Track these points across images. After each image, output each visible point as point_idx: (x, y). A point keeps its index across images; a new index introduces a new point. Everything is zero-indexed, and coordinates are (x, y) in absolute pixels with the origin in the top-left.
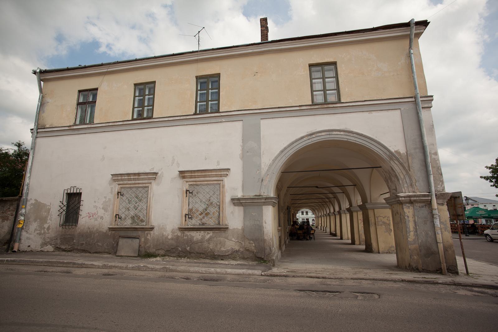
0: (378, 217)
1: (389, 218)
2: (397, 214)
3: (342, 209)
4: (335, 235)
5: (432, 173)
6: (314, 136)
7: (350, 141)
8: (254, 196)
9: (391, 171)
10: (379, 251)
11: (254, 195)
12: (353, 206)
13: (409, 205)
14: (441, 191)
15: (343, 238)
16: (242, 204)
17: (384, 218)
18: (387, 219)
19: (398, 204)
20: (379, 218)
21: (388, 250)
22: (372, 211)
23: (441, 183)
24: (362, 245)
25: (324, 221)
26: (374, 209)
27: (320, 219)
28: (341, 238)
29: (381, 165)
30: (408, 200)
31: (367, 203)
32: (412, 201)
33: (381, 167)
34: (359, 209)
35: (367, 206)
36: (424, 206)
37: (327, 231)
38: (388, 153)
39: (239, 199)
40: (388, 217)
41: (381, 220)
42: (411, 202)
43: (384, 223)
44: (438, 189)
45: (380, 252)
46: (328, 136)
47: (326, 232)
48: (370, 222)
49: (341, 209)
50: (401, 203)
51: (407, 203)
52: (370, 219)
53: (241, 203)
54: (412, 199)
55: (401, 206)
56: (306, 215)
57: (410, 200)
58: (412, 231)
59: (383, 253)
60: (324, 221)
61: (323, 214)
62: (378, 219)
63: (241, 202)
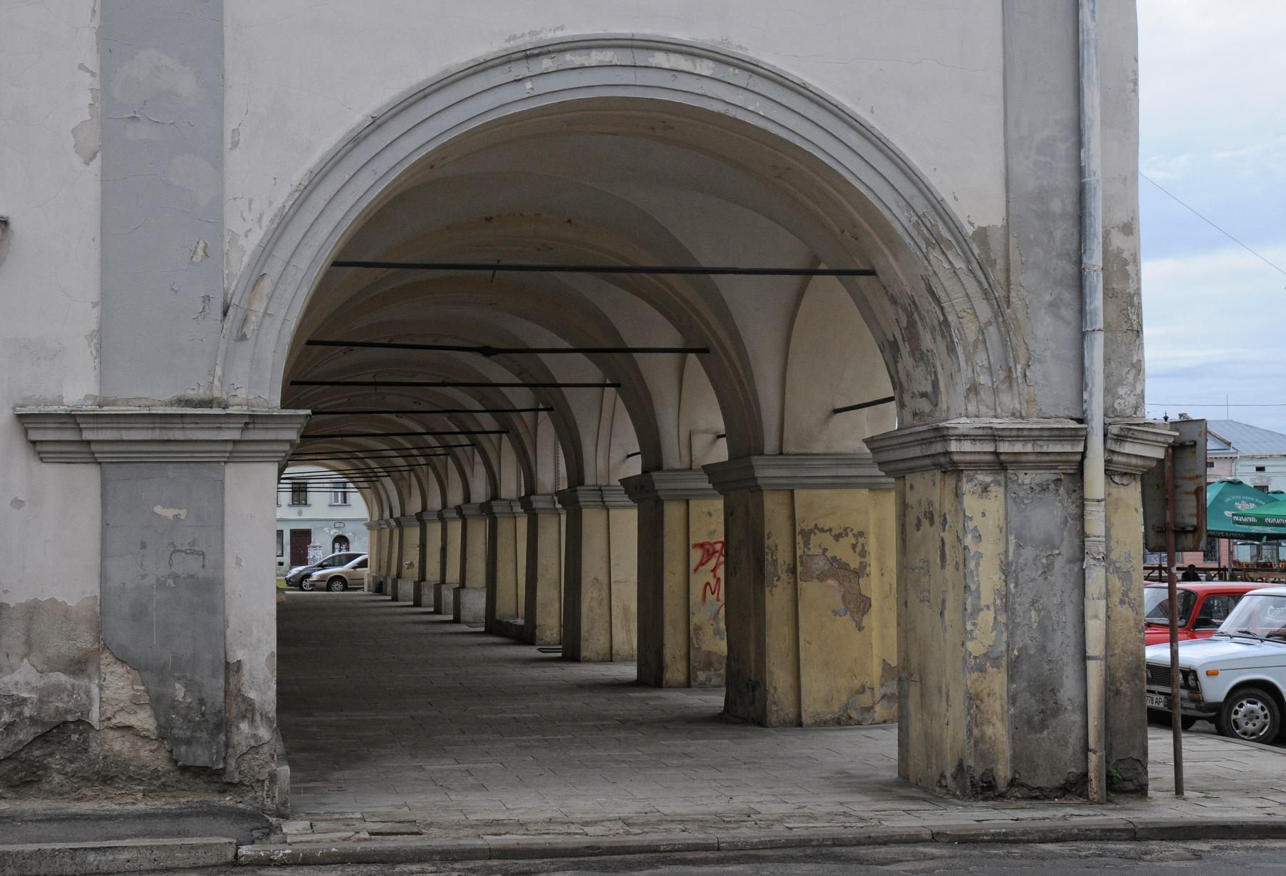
0: (807, 534)
1: (861, 540)
2: (925, 523)
3: (589, 480)
4: (525, 635)
5: (1100, 325)
6: (546, 64)
7: (741, 115)
8: (171, 404)
9: (925, 303)
10: (800, 715)
11: (171, 395)
12: (665, 467)
13: (988, 479)
14: (1129, 411)
16: (94, 448)
17: (837, 537)
18: (854, 547)
19: (938, 475)
20: (814, 539)
21: (846, 707)
22: (782, 498)
23: (1131, 377)
24: (704, 687)
25: (444, 550)
26: (792, 491)
27: (413, 534)
28: (572, 654)
29: (879, 265)
30: (985, 453)
31: (762, 454)
32: (1003, 458)
33: (872, 273)
34: (711, 486)
35: (759, 473)
36: (1052, 486)
37: (466, 614)
38: (920, 204)
39: (72, 419)
40: (861, 534)
41: (825, 550)
42: (1000, 465)
43: (838, 569)
44: (1116, 405)
45: (806, 719)
46: (627, 77)
47: (457, 620)
48: (768, 558)
49: (581, 482)
50: (952, 468)
51: (978, 466)
52: (767, 542)
53: (89, 442)
54: (1004, 447)
55: (951, 481)
56: (296, 509)
57: (996, 454)
58: (988, 607)
59: (822, 724)
60: (444, 550)
62: (807, 544)
63: (88, 435)
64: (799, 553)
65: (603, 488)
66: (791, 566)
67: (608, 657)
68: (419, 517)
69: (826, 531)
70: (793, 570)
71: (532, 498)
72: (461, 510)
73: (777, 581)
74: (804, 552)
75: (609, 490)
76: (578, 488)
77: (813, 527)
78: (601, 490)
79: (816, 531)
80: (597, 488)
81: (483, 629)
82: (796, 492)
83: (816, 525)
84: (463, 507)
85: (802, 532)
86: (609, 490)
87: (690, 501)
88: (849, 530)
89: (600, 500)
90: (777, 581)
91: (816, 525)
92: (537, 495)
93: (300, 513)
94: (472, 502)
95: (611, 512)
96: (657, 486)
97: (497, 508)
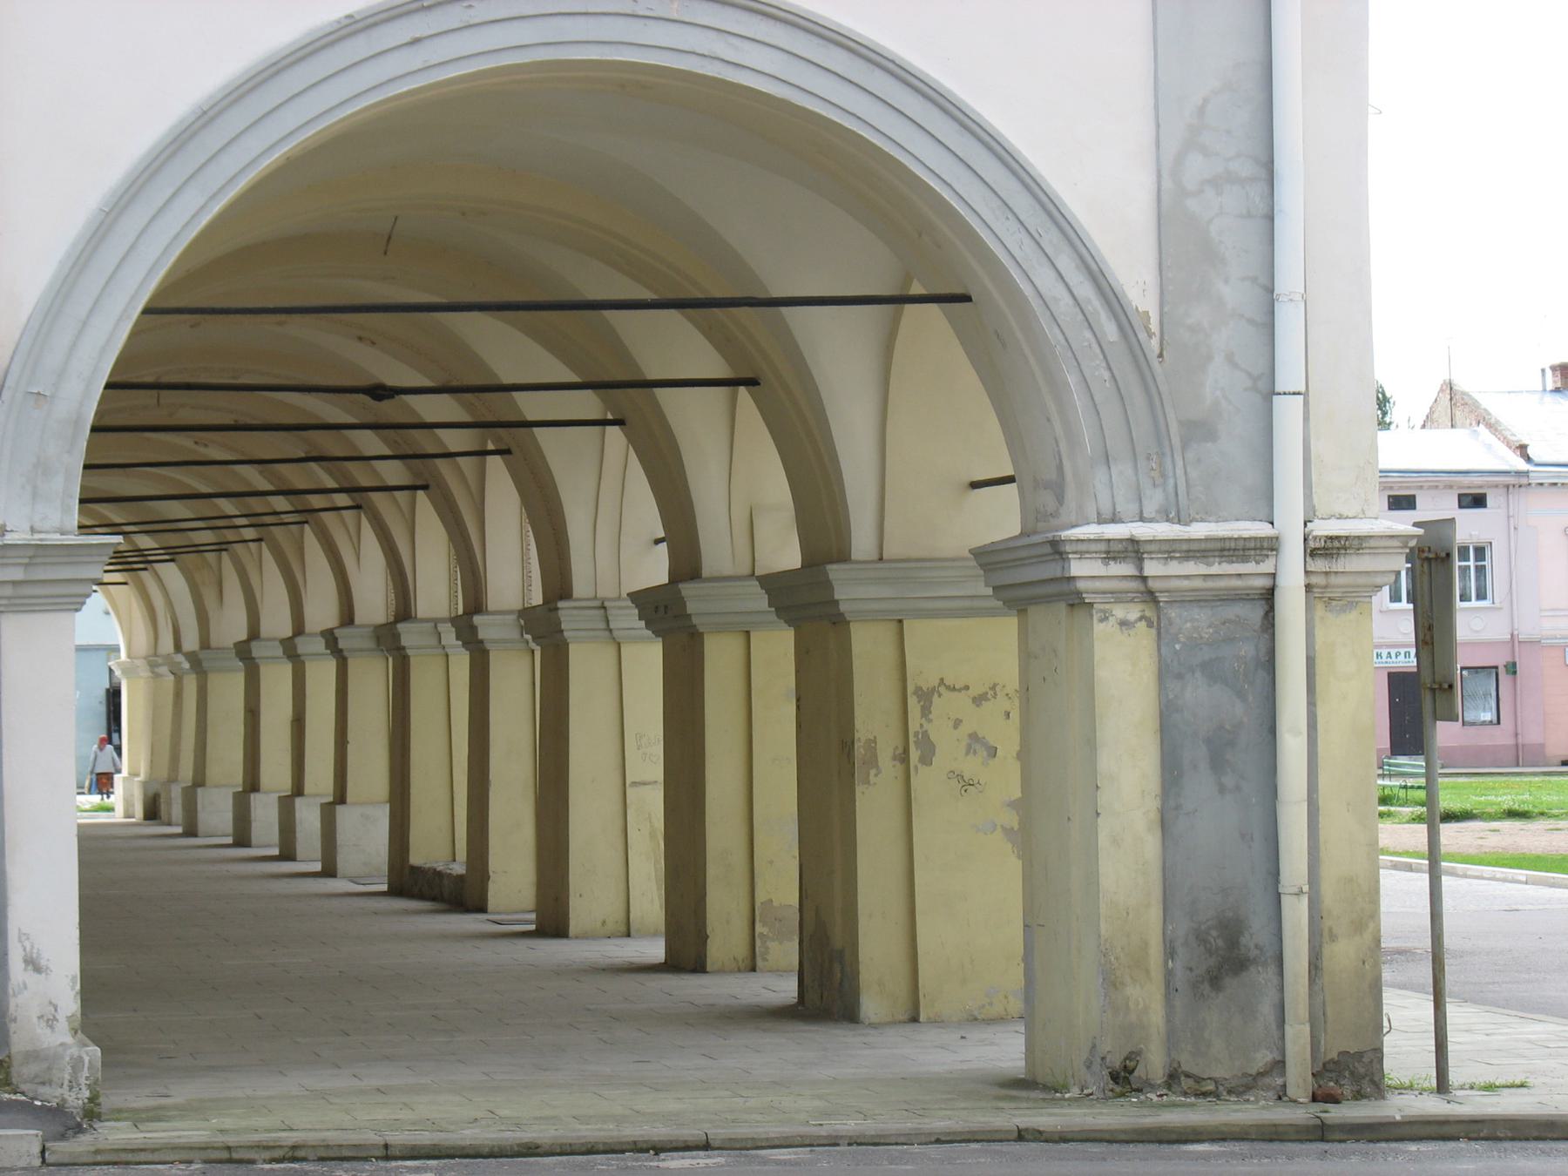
0: (926, 696)
3: (581, 585)
17: (978, 700)
24: (778, 971)
26: (900, 621)
27: (229, 690)
37: (344, 861)
47: (329, 871)
61: (277, 622)
62: (926, 711)
64: (914, 726)
65: (606, 604)
66: (900, 750)
67: (623, 929)
68: (243, 651)
69: (960, 690)
70: (904, 758)
71: (477, 619)
72: (336, 639)
73: (876, 775)
74: (921, 725)
76: (561, 604)
77: (936, 683)
78: (605, 608)
79: (942, 689)
80: (597, 603)
81: (385, 888)
82: (905, 623)
83: (942, 680)
84: (337, 633)
85: (919, 692)
87: (752, 634)
88: (998, 689)
89: (603, 625)
90: (876, 775)
91: (942, 680)
92: (487, 613)
94: (357, 621)
95: (626, 650)
96: (691, 608)
97: (409, 635)
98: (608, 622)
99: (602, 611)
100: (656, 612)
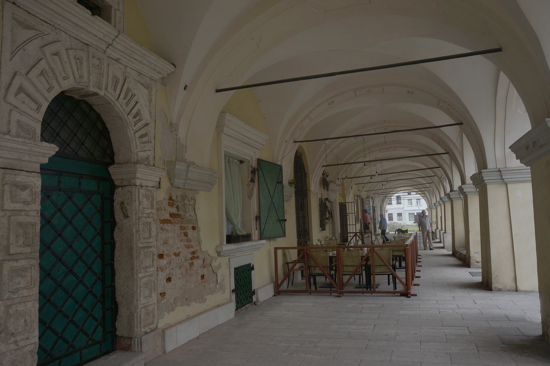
3: (491, 165)
15: (494, 285)
49: (485, 167)
65: (500, 170)
75: (506, 171)
78: (500, 171)
80: (498, 170)
86: (506, 171)
89: (500, 178)
93: (419, 208)
95: (509, 186)
98: (502, 176)
99: (499, 172)
100: (527, 150)
